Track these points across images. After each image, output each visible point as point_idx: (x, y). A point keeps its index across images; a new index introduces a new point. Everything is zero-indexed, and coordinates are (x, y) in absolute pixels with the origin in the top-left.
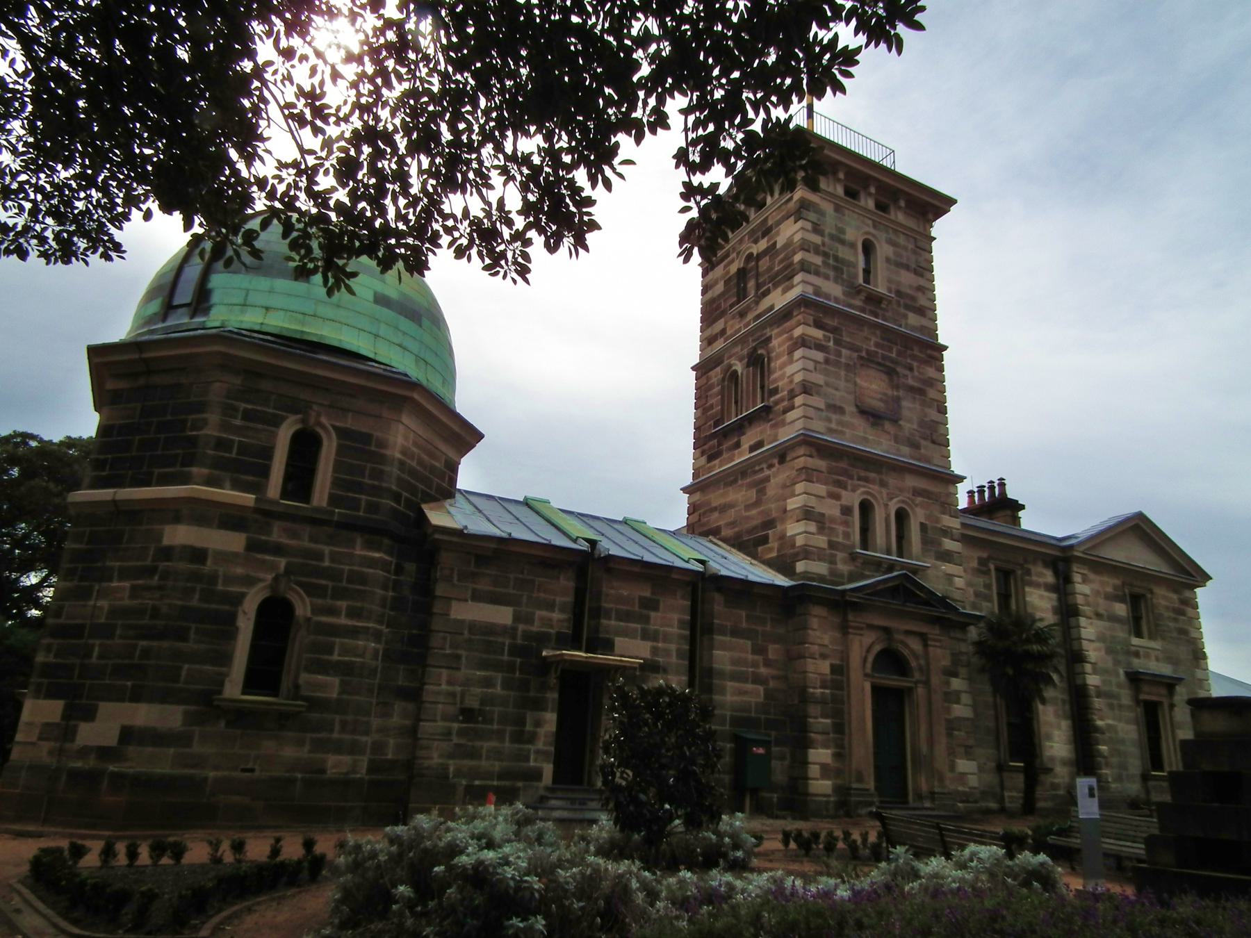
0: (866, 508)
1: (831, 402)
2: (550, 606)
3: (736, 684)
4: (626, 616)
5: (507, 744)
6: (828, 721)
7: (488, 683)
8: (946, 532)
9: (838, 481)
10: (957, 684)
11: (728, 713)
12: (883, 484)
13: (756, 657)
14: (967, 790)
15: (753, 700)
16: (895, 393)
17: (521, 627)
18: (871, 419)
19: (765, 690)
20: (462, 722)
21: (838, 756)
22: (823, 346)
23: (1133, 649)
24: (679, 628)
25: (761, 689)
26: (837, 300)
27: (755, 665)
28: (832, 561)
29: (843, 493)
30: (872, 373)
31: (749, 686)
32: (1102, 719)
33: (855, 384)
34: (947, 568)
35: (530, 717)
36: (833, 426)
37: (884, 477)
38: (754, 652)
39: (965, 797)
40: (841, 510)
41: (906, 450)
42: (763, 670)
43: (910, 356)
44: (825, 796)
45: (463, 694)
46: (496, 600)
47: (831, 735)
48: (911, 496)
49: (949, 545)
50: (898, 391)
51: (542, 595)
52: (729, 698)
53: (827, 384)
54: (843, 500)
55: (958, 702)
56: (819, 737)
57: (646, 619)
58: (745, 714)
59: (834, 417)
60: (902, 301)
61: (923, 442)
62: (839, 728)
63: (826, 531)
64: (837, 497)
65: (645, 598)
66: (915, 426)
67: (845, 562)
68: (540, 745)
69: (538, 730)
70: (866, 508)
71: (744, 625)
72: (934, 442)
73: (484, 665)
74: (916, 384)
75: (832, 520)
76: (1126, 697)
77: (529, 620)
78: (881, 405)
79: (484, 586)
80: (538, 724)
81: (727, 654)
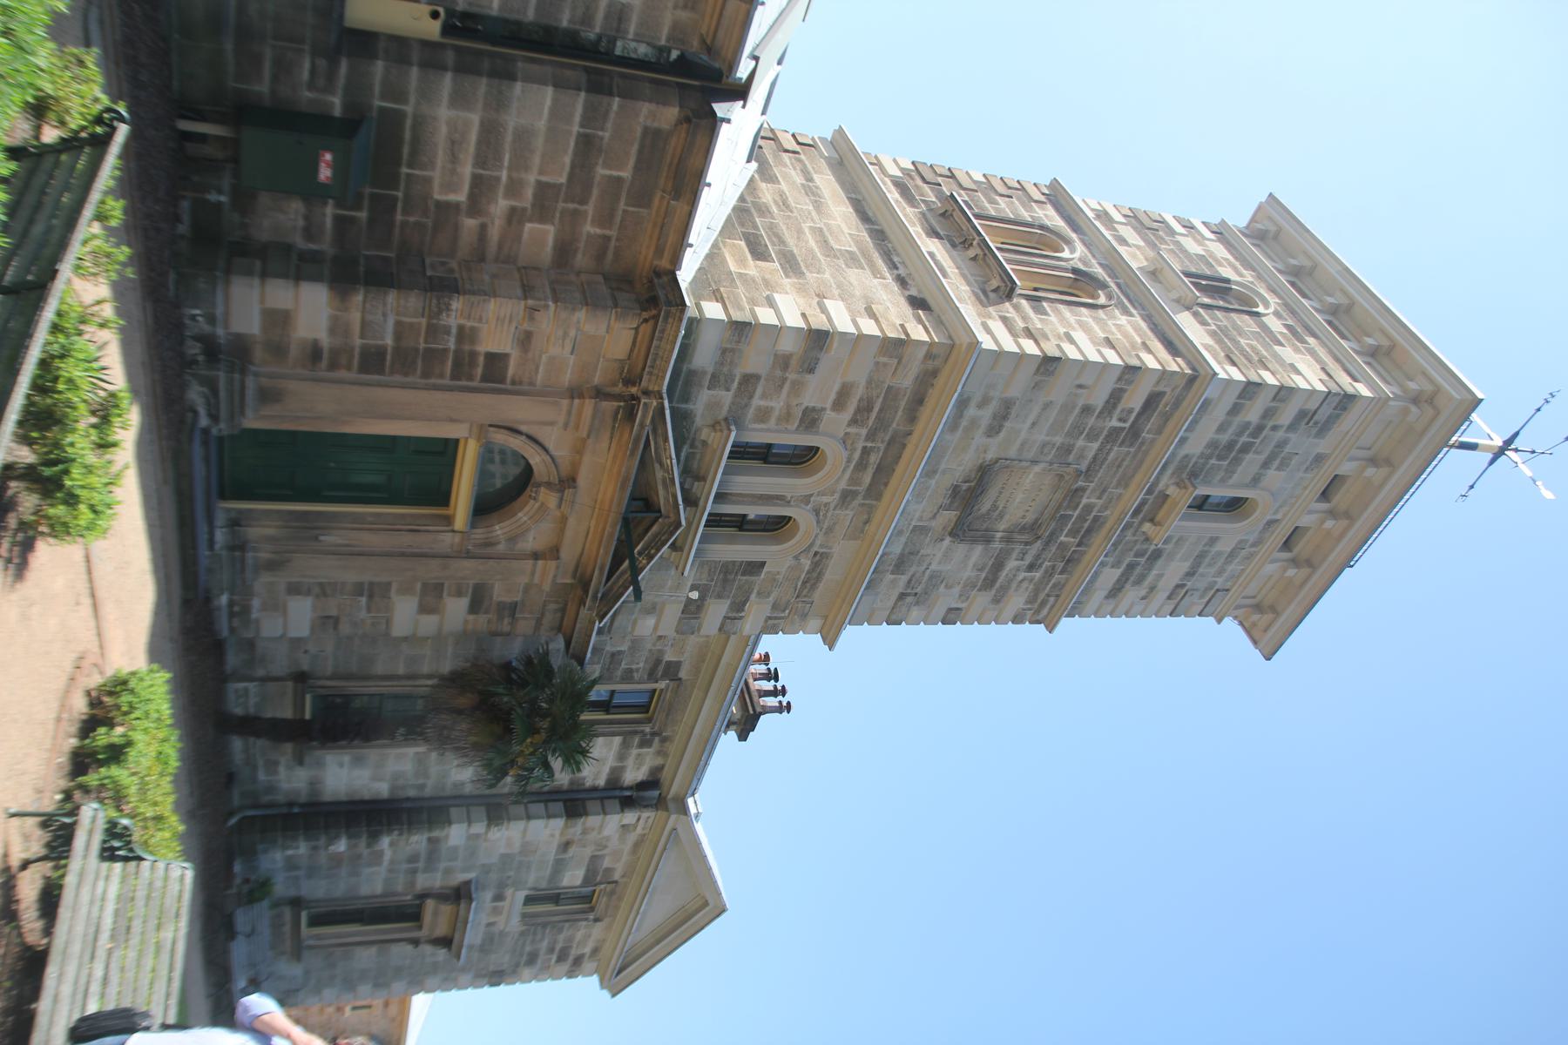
3: (473, 137)
6: (389, 341)
9: (869, 409)
10: (456, 609)
11: (409, 109)
12: (846, 497)
13: (529, 193)
14: (254, 615)
15: (437, 175)
19: (457, 206)
21: (314, 353)
22: (1115, 406)
25: (461, 197)
27: (514, 188)
28: (715, 381)
29: (847, 415)
31: (467, 170)
32: (392, 844)
33: (1034, 462)
36: (971, 411)
38: (542, 187)
39: (240, 612)
40: (814, 409)
43: (1053, 567)
44: (227, 314)
47: (358, 342)
48: (815, 549)
50: (1002, 540)
52: (443, 114)
54: (833, 414)
55: (424, 609)
56: (355, 317)
58: (406, 150)
59: (986, 415)
61: (904, 579)
62: (372, 361)
63: (778, 373)
64: (839, 404)
67: (713, 405)
71: (601, 171)
72: (902, 596)
75: (797, 388)
78: (984, 509)
81: (542, 124)
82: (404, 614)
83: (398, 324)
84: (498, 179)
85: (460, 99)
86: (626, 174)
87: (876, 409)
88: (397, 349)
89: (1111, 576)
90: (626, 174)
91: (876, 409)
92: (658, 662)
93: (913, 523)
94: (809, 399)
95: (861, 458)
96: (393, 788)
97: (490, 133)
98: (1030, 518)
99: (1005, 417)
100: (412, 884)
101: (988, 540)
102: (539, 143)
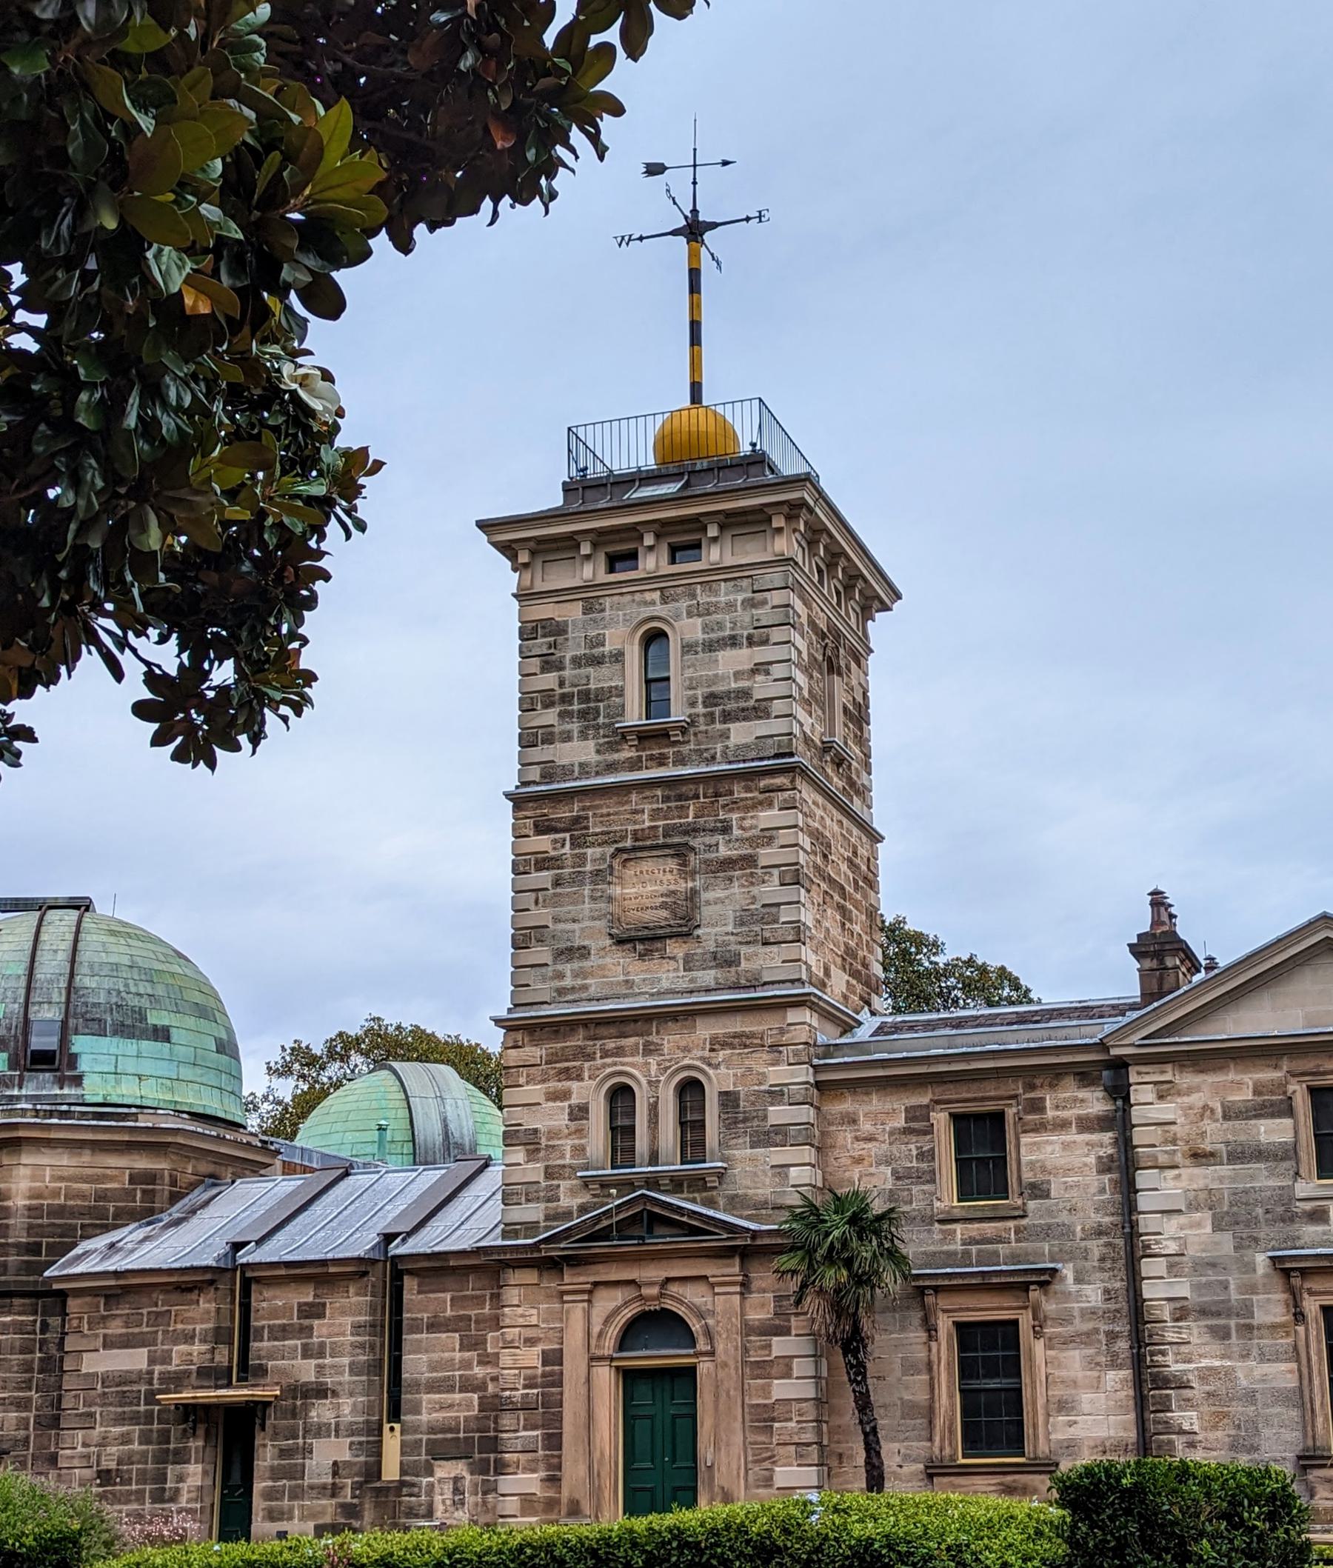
0: (621, 1095)
1: (562, 945)
2: (189, 1338)
4: (282, 1332)
5: (148, 1506)
7: (125, 1439)
8: (776, 1095)
9: (567, 1069)
10: (780, 1346)
11: (425, 1437)
12: (649, 1050)
13: (467, 1354)
16: (690, 885)
17: (158, 1369)
18: (640, 947)
20: (100, 1485)
21: (553, 1480)
23: (1308, 1206)
24: (352, 1334)
26: (584, 769)
27: (467, 1365)
29: (574, 1085)
30: (647, 866)
33: (610, 899)
34: (778, 1155)
35: (171, 1470)
36: (568, 982)
37: (654, 1038)
41: (708, 977)
42: (479, 1371)
45: (99, 1456)
46: (127, 1342)
47: (541, 1452)
48: (707, 1054)
49: (778, 1114)
50: (694, 880)
51: (180, 1326)
52: (424, 1417)
53: (557, 920)
54: (574, 1096)
57: (307, 1331)
58: (449, 1436)
59: (567, 968)
60: (717, 710)
61: (744, 950)
62: (554, 1442)
63: (542, 1154)
64: (565, 1095)
65: (306, 1304)
66: (730, 928)
67: (573, 1193)
68: (183, 1502)
69: (181, 1485)
70: (621, 1095)
72: (766, 943)
73: (120, 1420)
74: (734, 853)
75: (553, 1134)
76: (1271, 1309)
77: (166, 1359)
78: (664, 913)
79: (116, 1328)
80: (181, 1479)
82: (781, 1389)
83: (525, 1429)
84: (461, 1376)
85: (416, 1410)
86: (448, 1296)
87: (566, 1064)
88: (543, 1427)
89: (741, 733)
90: (448, 1296)
91: (566, 1064)
92: (906, 1131)
93: (682, 973)
94: (562, 1120)
95: (611, 1056)
96: (1114, 1364)
97: (433, 1387)
98: (672, 864)
99: (570, 949)
100: (1274, 1327)
101: (694, 893)
102: (435, 1356)
